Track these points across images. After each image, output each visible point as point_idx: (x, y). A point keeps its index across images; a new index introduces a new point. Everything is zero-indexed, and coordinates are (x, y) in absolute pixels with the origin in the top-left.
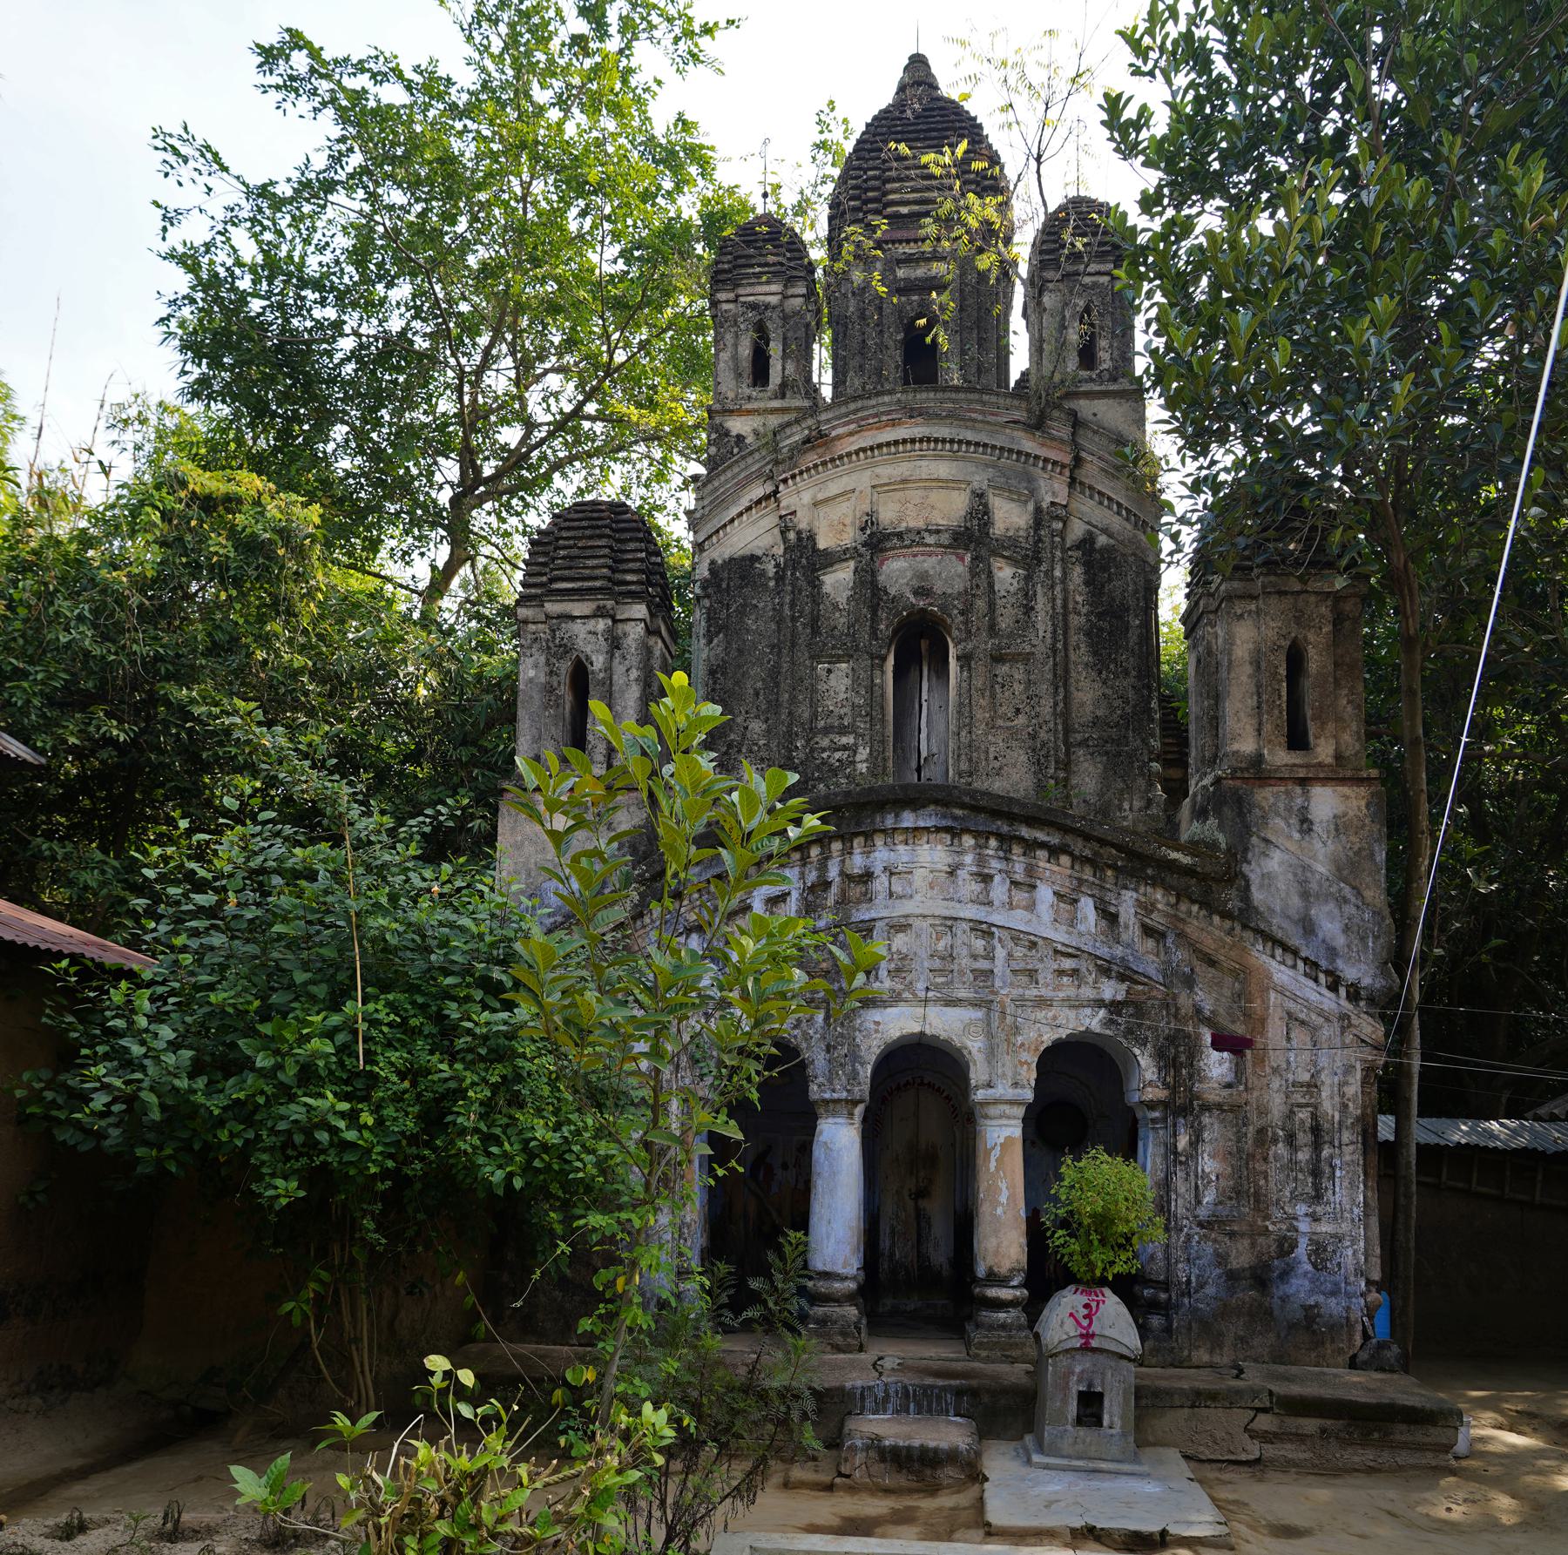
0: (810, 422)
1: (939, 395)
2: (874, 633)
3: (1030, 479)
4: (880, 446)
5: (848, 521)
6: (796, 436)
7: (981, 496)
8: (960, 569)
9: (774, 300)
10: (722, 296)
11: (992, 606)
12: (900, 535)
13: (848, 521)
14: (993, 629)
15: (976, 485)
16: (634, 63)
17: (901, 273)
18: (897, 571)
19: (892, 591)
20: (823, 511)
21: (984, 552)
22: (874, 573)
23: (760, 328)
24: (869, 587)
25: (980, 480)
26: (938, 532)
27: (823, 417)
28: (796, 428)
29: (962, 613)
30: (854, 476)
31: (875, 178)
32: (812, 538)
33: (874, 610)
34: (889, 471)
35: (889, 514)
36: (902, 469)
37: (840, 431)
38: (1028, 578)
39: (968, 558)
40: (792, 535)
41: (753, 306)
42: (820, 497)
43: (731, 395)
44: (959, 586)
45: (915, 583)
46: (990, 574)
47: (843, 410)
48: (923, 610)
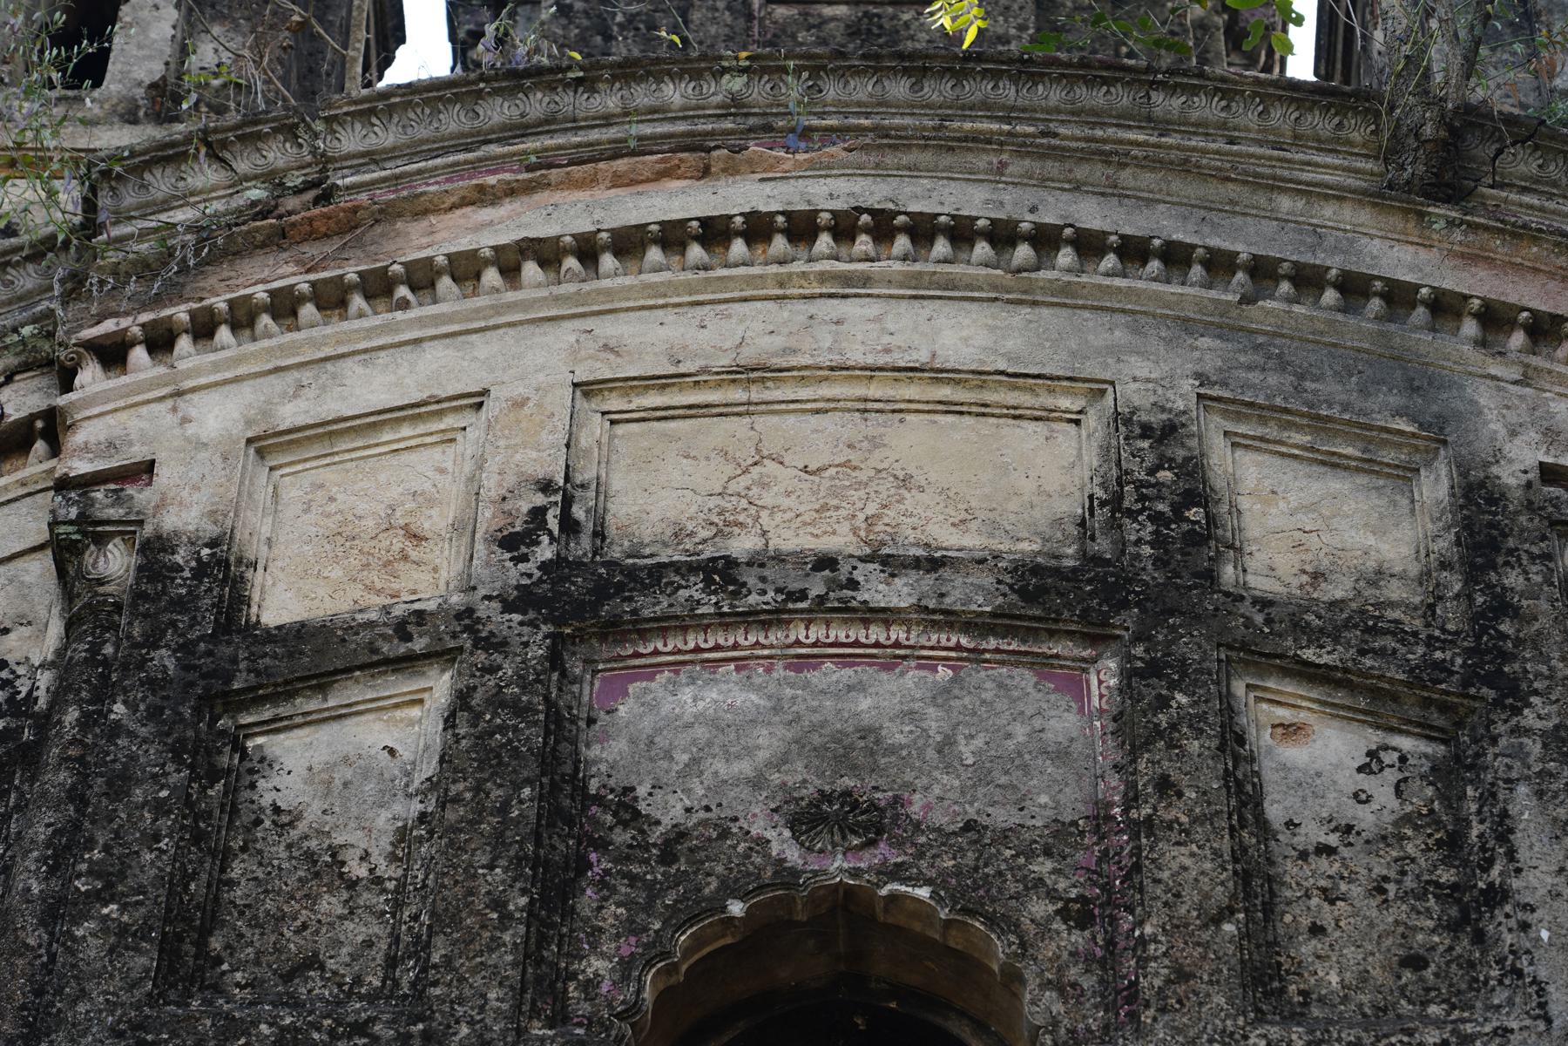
0: (277, 154)
2: (543, 986)
3: (1419, 382)
4: (629, 243)
5: (436, 521)
6: (206, 192)
7: (1168, 431)
8: (1063, 723)
11: (1255, 884)
12: (722, 573)
13: (436, 521)
14: (1265, 982)
15: (1134, 394)
18: (694, 733)
19: (669, 811)
20: (299, 482)
21: (1190, 646)
22: (562, 730)
24: (530, 791)
25: (1154, 375)
26: (933, 563)
27: (351, 140)
29: (1079, 914)
30: (483, 347)
32: (224, 569)
33: (554, 889)
34: (658, 329)
35: (658, 495)
36: (754, 330)
38: (1450, 774)
39: (1105, 676)
40: (115, 563)
42: (291, 414)
44: (1053, 797)
45: (804, 778)
46: (1232, 741)
48: (847, 907)
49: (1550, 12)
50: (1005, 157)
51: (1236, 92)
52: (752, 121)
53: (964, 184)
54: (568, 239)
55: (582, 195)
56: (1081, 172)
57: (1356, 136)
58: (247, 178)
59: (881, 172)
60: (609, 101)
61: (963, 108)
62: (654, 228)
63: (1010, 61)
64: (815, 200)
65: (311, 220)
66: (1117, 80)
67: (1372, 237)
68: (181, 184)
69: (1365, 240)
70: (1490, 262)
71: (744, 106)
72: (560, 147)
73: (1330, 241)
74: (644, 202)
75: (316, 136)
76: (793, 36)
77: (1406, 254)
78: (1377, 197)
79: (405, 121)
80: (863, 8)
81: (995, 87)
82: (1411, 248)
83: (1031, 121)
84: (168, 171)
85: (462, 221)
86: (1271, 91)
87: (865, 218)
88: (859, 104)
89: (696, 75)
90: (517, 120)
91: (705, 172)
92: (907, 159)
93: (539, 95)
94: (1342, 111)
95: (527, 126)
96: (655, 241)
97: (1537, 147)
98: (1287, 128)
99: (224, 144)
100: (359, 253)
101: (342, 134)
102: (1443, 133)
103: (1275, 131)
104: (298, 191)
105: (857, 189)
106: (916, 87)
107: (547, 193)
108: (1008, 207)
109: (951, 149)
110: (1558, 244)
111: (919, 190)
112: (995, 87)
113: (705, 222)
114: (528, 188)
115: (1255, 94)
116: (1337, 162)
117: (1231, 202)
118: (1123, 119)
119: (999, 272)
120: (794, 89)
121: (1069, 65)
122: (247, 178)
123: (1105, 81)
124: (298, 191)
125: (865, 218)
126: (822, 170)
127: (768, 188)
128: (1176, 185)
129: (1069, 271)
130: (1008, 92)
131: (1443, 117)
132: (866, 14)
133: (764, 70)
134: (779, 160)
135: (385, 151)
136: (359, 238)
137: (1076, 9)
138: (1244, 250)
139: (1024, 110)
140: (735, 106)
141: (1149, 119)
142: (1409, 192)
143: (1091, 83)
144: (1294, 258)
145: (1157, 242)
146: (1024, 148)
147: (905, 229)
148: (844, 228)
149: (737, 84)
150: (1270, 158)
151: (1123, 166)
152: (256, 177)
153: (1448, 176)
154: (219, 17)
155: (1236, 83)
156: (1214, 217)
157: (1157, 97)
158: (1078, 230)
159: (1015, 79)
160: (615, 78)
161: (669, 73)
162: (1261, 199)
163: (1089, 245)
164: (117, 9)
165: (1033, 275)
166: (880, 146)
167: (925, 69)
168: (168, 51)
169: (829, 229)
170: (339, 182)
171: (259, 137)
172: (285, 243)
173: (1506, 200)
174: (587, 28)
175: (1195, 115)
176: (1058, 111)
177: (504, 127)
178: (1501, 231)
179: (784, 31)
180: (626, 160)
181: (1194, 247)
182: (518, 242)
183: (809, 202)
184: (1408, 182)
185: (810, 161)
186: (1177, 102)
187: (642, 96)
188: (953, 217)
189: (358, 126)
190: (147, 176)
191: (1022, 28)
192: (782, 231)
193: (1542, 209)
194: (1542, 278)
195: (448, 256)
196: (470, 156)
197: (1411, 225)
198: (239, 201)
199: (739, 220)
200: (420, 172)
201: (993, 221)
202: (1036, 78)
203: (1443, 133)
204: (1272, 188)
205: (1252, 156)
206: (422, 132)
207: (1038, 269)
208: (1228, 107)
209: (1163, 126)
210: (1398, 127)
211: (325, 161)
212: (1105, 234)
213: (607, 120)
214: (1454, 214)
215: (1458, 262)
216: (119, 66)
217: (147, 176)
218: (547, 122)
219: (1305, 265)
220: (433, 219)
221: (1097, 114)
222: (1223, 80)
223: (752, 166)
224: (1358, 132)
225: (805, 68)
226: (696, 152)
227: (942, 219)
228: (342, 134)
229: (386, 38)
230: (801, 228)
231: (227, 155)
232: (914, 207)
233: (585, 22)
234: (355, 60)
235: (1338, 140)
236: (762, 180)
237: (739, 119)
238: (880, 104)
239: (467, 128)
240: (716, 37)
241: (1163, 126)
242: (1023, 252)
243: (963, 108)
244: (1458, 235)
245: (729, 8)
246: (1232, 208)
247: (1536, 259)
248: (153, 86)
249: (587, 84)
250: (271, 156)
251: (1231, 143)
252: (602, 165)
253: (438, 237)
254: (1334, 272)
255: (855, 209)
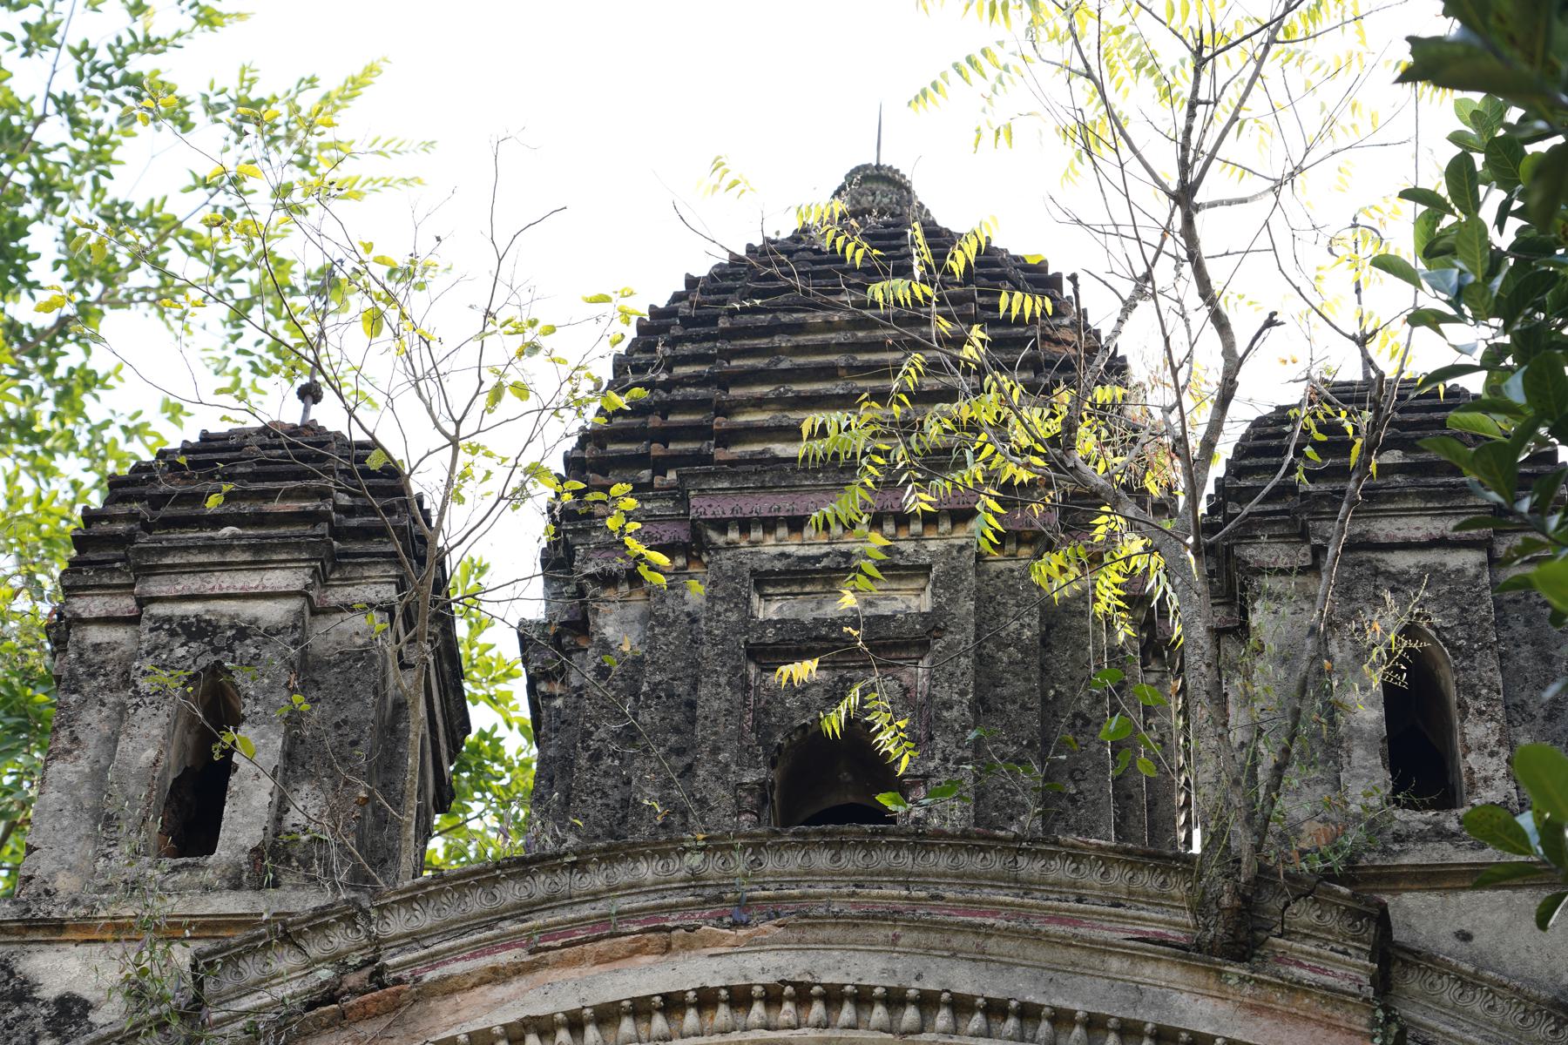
0: (340, 939)
1: (852, 861)
9: (273, 612)
10: (91, 605)
16: (100, 362)
17: (768, 610)
23: (217, 706)
27: (397, 924)
28: (286, 961)
31: (698, 381)
37: (457, 968)
41: (196, 630)
43: (65, 884)
47: (477, 903)
49: (1351, 738)
50: (898, 930)
51: (1084, 856)
52: (708, 892)
53: (866, 955)
54: (560, 1016)
55: (573, 973)
56: (957, 941)
57: (1176, 892)
58: (318, 961)
59: (802, 946)
60: (596, 880)
61: (872, 874)
62: (626, 1003)
63: (908, 835)
64: (750, 975)
65: (364, 1004)
66: (992, 848)
67: (1181, 992)
68: (267, 969)
69: (1176, 995)
70: (1271, 1011)
71: (702, 879)
72: (558, 923)
73: (1148, 997)
74: (619, 979)
75: (371, 922)
76: (782, 702)
77: (1206, 1006)
78: (1189, 952)
79: (439, 905)
80: (839, 672)
81: (897, 856)
82: (1211, 1001)
83: (925, 885)
84: (257, 958)
85: (480, 999)
86: (1111, 855)
87: (789, 990)
88: (791, 874)
89: (664, 855)
90: (525, 899)
91: (667, 948)
92: (822, 934)
93: (543, 877)
94: (1166, 871)
95: (534, 904)
96: (627, 1014)
97: (1316, 901)
98: (1123, 886)
99: (300, 934)
100: (401, 1032)
101: (391, 919)
102: (1237, 903)
103: (1114, 889)
104: (357, 969)
105: (783, 963)
106: (835, 859)
107: (546, 971)
108: (899, 975)
109: (856, 925)
110: (1324, 997)
111: (831, 962)
112: (897, 856)
113: (666, 997)
114: (532, 968)
115: (1098, 858)
116: (1160, 916)
117: (1073, 964)
118: (996, 881)
119: (890, 1036)
120: (740, 863)
121: (953, 836)
122: (318, 961)
123: (982, 849)
124: (357, 969)
125: (789, 990)
126: (756, 945)
127: (714, 962)
128: (1031, 950)
129: (945, 1033)
130: (906, 861)
131: (1237, 888)
132: (841, 677)
133: (717, 848)
134: (724, 936)
135: (424, 931)
136: (401, 1017)
137: (1011, 663)
138: (1080, 1008)
139: (919, 875)
140: (695, 877)
141: (1016, 880)
142: (1210, 953)
143: (971, 851)
144: (1119, 1014)
145: (1013, 1004)
146: (914, 925)
147: (820, 997)
148: (772, 997)
149: (695, 860)
150: (1109, 915)
151: (989, 936)
152: (324, 960)
153: (1242, 936)
154: (311, 776)
155: (1083, 849)
156: (1058, 976)
157: (1023, 861)
158: (953, 995)
159: (912, 849)
160: (601, 860)
161: (643, 854)
162: (1096, 961)
163: (961, 1006)
164: (228, 779)
165: (916, 1038)
166: (801, 925)
167: (842, 842)
168: (266, 817)
169: (760, 999)
170: (389, 962)
171: (327, 925)
172: (345, 1023)
173: (1290, 948)
174: (622, 690)
175: (1051, 877)
176: (945, 875)
177: (516, 907)
178: (1280, 986)
179: (775, 697)
180: (606, 942)
181: (1042, 1006)
182: (521, 1020)
183: (745, 977)
184: (1211, 942)
185: (750, 936)
186: (1038, 865)
187: (622, 874)
188: (857, 986)
189: (403, 911)
190: (241, 963)
191: (963, 693)
192: (725, 1002)
193: (1318, 956)
194: (1311, 1026)
195: (469, 1034)
196: (489, 934)
197: (1211, 981)
198: (312, 982)
199: (691, 995)
200: (450, 950)
201: (887, 989)
202: (928, 848)
203: (1237, 903)
204: (1105, 952)
205: (1094, 913)
206: (452, 914)
207: (921, 1031)
208: (1078, 868)
209: (1026, 886)
210: (1204, 893)
211: (377, 943)
212: (974, 997)
213: (595, 896)
214: (1244, 972)
215: (1247, 1013)
216: (228, 834)
217: (241, 963)
218: (549, 900)
219: (1128, 1020)
220: (458, 997)
221: (975, 877)
222: (1073, 846)
223: (704, 942)
224: (1178, 888)
225: (749, 845)
226: (662, 938)
227: (848, 988)
228: (391, 919)
229: (454, 732)
230: (740, 998)
231: (302, 943)
232: (826, 979)
233: (621, 684)
234: (409, 824)
235: (1162, 896)
236: (711, 956)
237: (698, 891)
238: (807, 874)
239: (486, 909)
240: (718, 712)
241: (1026, 886)
242: (910, 1015)
243: (872, 874)
244: (1247, 990)
245: (729, 683)
246: (1074, 969)
247: (1308, 1009)
248: (254, 850)
249: (580, 866)
250: (336, 941)
251: (1079, 901)
252: (588, 947)
253: (462, 1015)
254: (1149, 1026)
255: (781, 982)
